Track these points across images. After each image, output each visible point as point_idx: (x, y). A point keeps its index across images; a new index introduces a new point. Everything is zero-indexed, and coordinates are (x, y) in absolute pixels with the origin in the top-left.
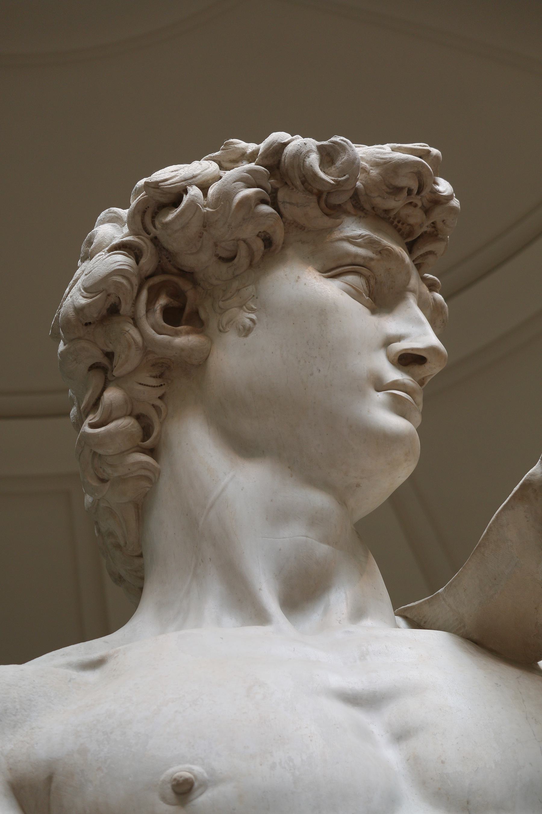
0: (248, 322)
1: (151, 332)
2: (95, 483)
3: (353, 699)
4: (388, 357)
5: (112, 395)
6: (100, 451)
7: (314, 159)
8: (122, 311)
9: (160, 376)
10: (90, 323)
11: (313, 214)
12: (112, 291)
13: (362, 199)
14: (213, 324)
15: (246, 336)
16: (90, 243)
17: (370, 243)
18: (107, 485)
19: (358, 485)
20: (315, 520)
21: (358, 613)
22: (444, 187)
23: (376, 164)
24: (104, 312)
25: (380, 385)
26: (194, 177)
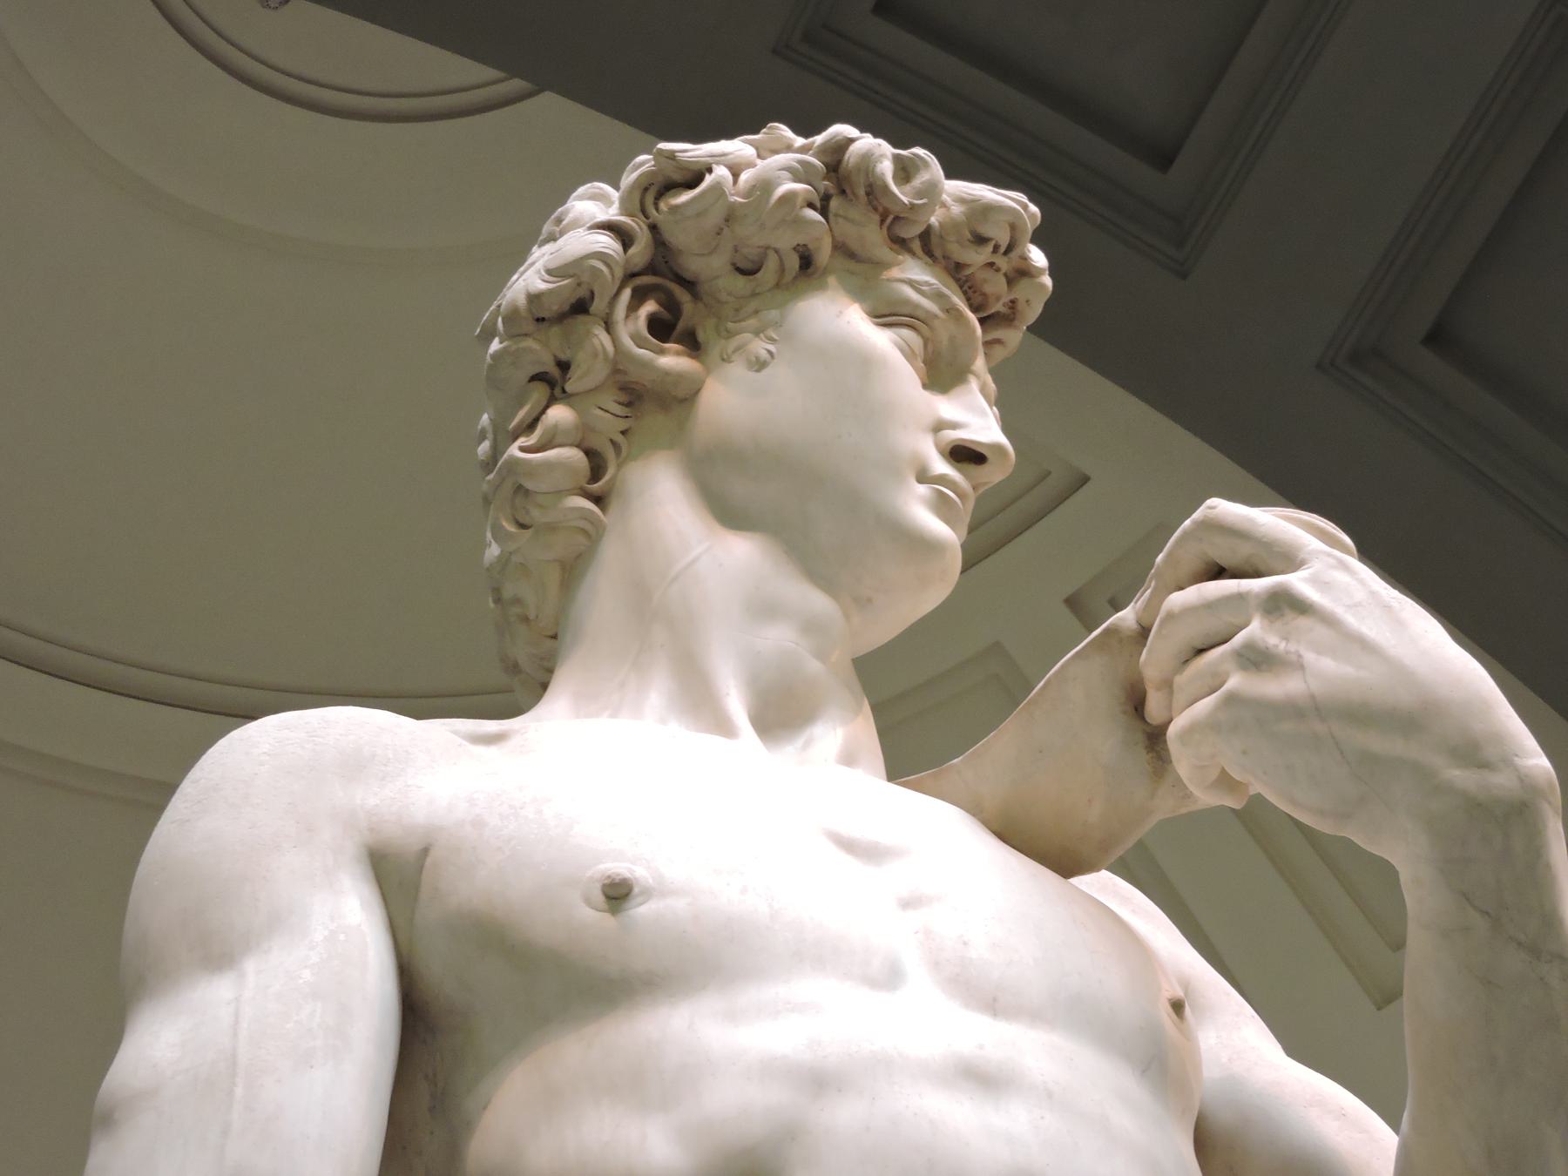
0: (764, 354)
1: (628, 342)
2: (512, 528)
4: (937, 445)
5: (559, 414)
6: (529, 485)
7: (886, 168)
8: (593, 309)
9: (629, 405)
10: (543, 319)
11: (872, 237)
12: (585, 278)
13: (934, 240)
15: (758, 371)
16: (559, 221)
18: (528, 533)
19: (869, 600)
20: (811, 627)
21: (848, 758)
23: (961, 200)
24: (566, 308)
25: (923, 477)
26: (724, 155)
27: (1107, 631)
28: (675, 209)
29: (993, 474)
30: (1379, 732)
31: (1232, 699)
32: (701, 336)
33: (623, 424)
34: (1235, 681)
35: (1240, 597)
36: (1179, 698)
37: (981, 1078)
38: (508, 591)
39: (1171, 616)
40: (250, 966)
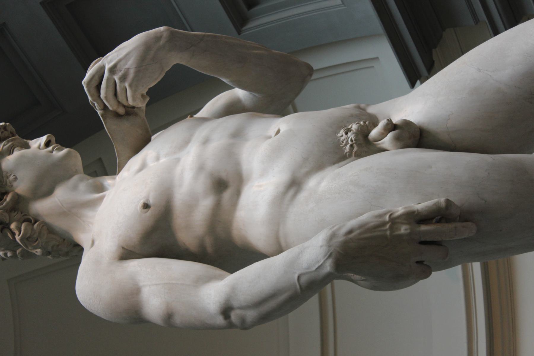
0: (14, 177)
5: (13, 226)
9: (15, 211)
14: (8, 188)
18: (39, 239)
20: (81, 180)
27: (102, 116)
29: (53, 139)
30: (147, 57)
32: (4, 191)
33: (20, 213)
35: (108, 79)
36: (124, 102)
37: (206, 141)
38: (50, 249)
39: (106, 98)
40: (141, 284)
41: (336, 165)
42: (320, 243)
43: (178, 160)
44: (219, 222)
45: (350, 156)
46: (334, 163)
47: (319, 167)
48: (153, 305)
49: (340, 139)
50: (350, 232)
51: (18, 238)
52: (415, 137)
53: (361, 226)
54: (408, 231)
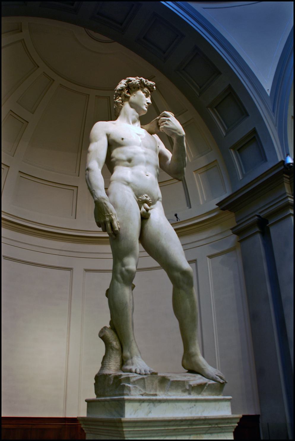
1: (125, 93)
3: (138, 134)
5: (120, 98)
7: (145, 82)
17: (147, 91)
20: (136, 116)
21: (138, 126)
22: (155, 87)
28: (130, 84)
29: (150, 105)
31: (164, 127)
34: (165, 125)
35: (166, 119)
37: (145, 153)
40: (98, 142)
41: (135, 195)
42: (102, 195)
43: (140, 146)
44: (119, 161)
45: (138, 199)
46: (135, 194)
47: (134, 190)
48: (92, 147)
49: (143, 195)
50: (105, 204)
51: (117, 100)
52: (145, 217)
53: (107, 207)
54: (107, 220)
